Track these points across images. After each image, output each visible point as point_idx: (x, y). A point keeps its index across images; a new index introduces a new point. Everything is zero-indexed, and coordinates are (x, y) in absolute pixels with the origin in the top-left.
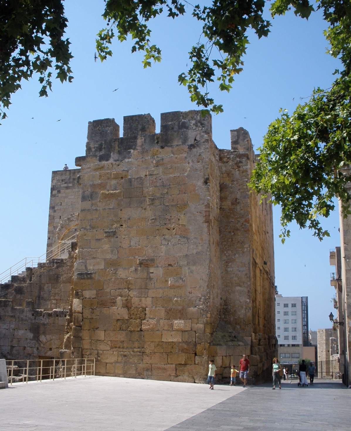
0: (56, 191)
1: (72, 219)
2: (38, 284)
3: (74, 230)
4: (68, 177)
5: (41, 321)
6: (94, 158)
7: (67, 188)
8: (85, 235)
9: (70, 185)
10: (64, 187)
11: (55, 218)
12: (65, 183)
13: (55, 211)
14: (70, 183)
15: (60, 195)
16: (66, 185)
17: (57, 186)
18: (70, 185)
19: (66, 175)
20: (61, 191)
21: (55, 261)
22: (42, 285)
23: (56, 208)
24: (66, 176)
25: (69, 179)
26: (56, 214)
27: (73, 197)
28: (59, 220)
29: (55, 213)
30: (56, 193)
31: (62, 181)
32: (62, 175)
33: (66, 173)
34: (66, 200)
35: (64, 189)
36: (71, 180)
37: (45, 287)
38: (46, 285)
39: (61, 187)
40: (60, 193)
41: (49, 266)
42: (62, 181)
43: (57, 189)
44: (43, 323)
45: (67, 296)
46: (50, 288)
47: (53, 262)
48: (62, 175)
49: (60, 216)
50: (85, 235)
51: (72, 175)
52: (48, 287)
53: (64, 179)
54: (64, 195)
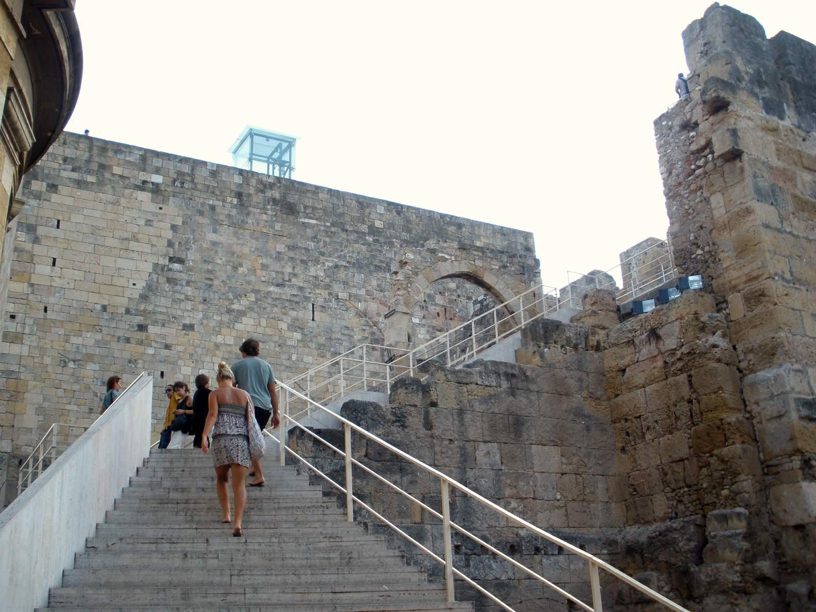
0: (45, 184)
1: (440, 255)
2: (456, 442)
3: (98, 307)
4: (86, 156)
5: (487, 570)
6: (754, 100)
7: (80, 184)
8: (786, 295)
9: (91, 179)
10: (70, 179)
11: (36, 259)
12: (73, 170)
13: (36, 240)
14: (89, 172)
15: (54, 197)
16: (75, 175)
17: (46, 171)
18: (91, 179)
19: (76, 149)
20: (60, 187)
21: (503, 370)
22: (469, 447)
23: (40, 231)
24: (78, 153)
25: (88, 161)
26: (38, 249)
27: (97, 214)
28: (50, 268)
29: (36, 246)
30: (44, 189)
31: (65, 160)
32: (65, 143)
33: (78, 143)
34: (76, 218)
35: (71, 185)
36: (94, 166)
37: (480, 454)
38: (483, 448)
39: (59, 176)
40: (56, 192)
41: (487, 383)
42: (65, 160)
43: (48, 178)
44: (497, 579)
45: (553, 488)
46: (498, 457)
47: (498, 375)
48: (65, 143)
49: (54, 260)
50: (786, 295)
51: (95, 151)
52: (488, 453)
53: (72, 158)
54: (69, 201)
